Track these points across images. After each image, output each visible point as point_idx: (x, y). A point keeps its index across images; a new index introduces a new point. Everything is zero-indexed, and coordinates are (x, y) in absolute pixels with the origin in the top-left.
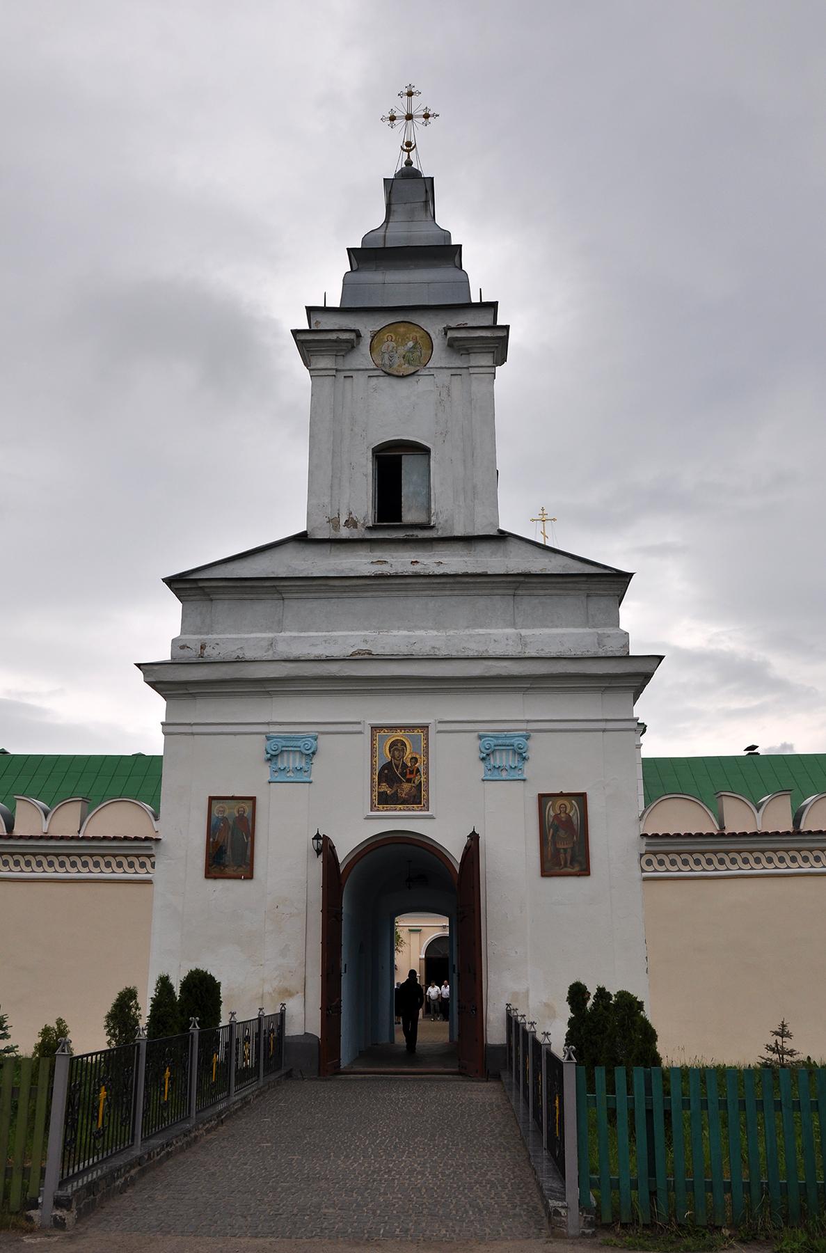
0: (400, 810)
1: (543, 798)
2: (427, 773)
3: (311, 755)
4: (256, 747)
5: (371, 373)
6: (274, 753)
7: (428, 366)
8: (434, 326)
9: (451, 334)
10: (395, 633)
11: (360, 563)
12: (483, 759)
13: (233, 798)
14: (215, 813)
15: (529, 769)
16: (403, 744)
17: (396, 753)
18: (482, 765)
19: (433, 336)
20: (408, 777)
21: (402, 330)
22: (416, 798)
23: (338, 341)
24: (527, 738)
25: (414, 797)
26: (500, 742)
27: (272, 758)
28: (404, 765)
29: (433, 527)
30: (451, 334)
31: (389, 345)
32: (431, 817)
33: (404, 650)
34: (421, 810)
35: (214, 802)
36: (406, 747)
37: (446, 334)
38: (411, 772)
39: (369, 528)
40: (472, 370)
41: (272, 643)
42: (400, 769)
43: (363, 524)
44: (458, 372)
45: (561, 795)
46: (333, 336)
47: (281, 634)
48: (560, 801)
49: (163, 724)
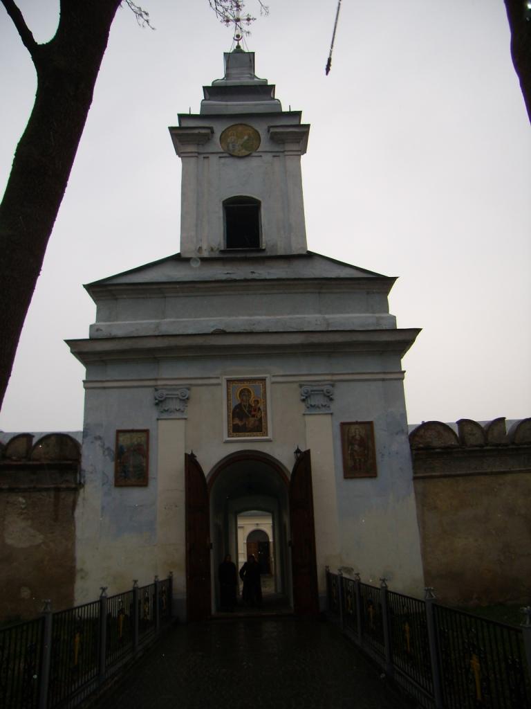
1: (343, 425)
3: (185, 400)
4: (147, 396)
5: (221, 155)
6: (160, 399)
7: (259, 149)
8: (261, 128)
9: (272, 130)
10: (241, 318)
11: (219, 272)
12: (303, 400)
13: (133, 431)
15: (334, 407)
16: (249, 391)
17: (244, 398)
18: (303, 405)
19: (260, 133)
20: (253, 413)
21: (240, 128)
23: (199, 134)
24: (333, 386)
26: (315, 388)
29: (264, 250)
30: (272, 130)
32: (269, 441)
33: (248, 329)
35: (121, 434)
37: (269, 131)
38: (255, 410)
39: (222, 252)
40: (286, 153)
41: (158, 326)
43: (218, 249)
44: (278, 154)
45: (357, 423)
46: (196, 131)
47: (163, 320)
48: (357, 426)
49: (84, 381)
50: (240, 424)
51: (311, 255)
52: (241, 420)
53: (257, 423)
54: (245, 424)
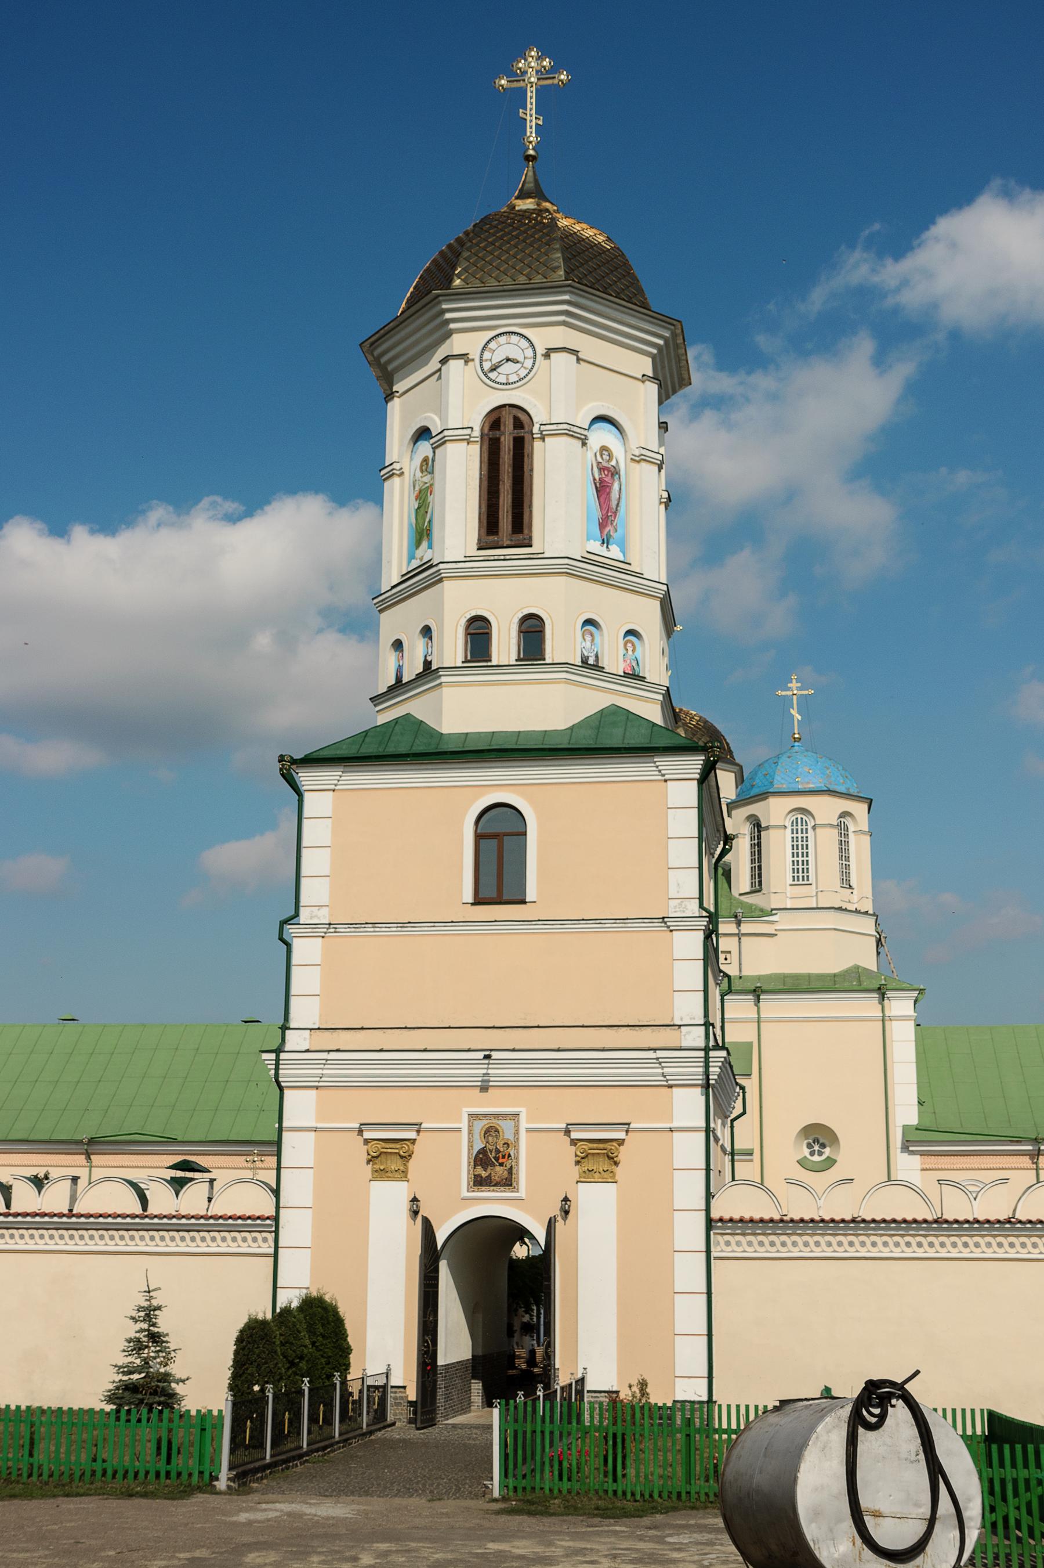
0: (493, 1191)
2: (517, 1158)
16: (497, 1131)
17: (490, 1139)
20: (501, 1161)
22: (508, 1182)
25: (506, 1179)
28: (498, 1151)
34: (512, 1191)
36: (498, 1132)
38: (503, 1157)
42: (493, 1154)
50: (484, 1174)
52: (485, 1170)
53: (506, 1172)
54: (490, 1175)
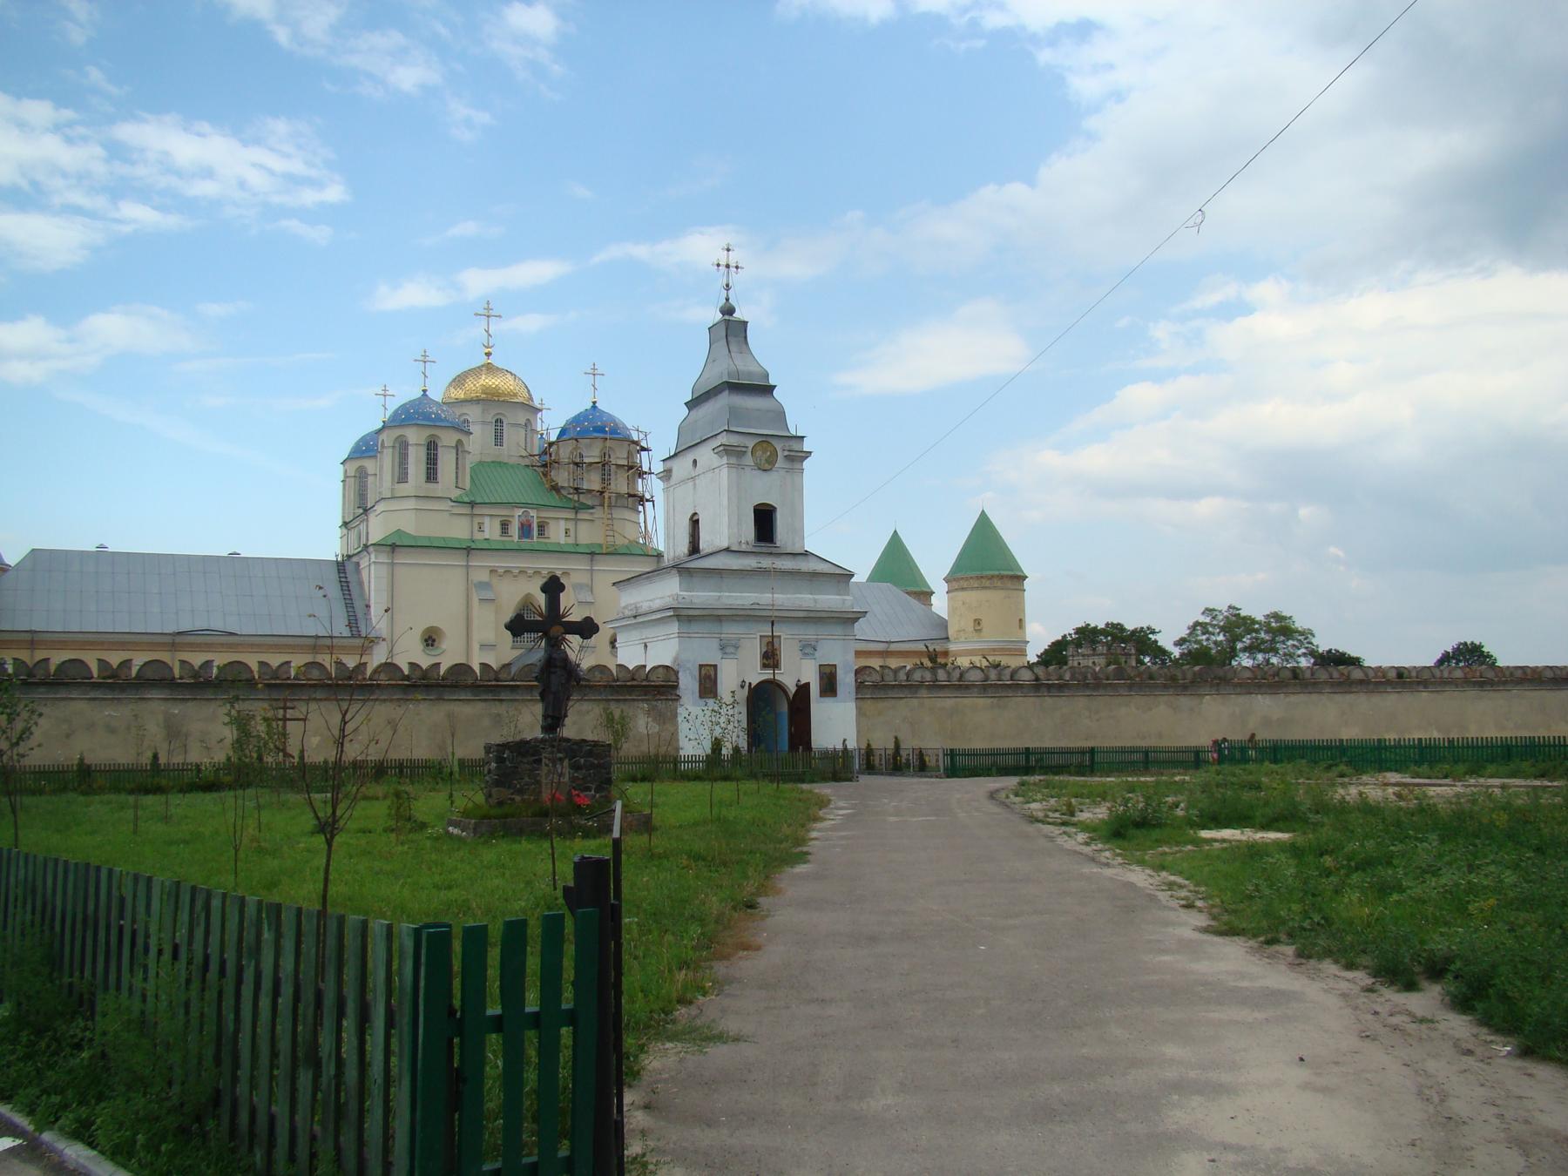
1: (820, 665)
3: (737, 648)
4: (715, 644)
11: (751, 563)
14: (703, 672)
21: (765, 445)
27: (722, 648)
31: (759, 453)
51: (806, 554)
